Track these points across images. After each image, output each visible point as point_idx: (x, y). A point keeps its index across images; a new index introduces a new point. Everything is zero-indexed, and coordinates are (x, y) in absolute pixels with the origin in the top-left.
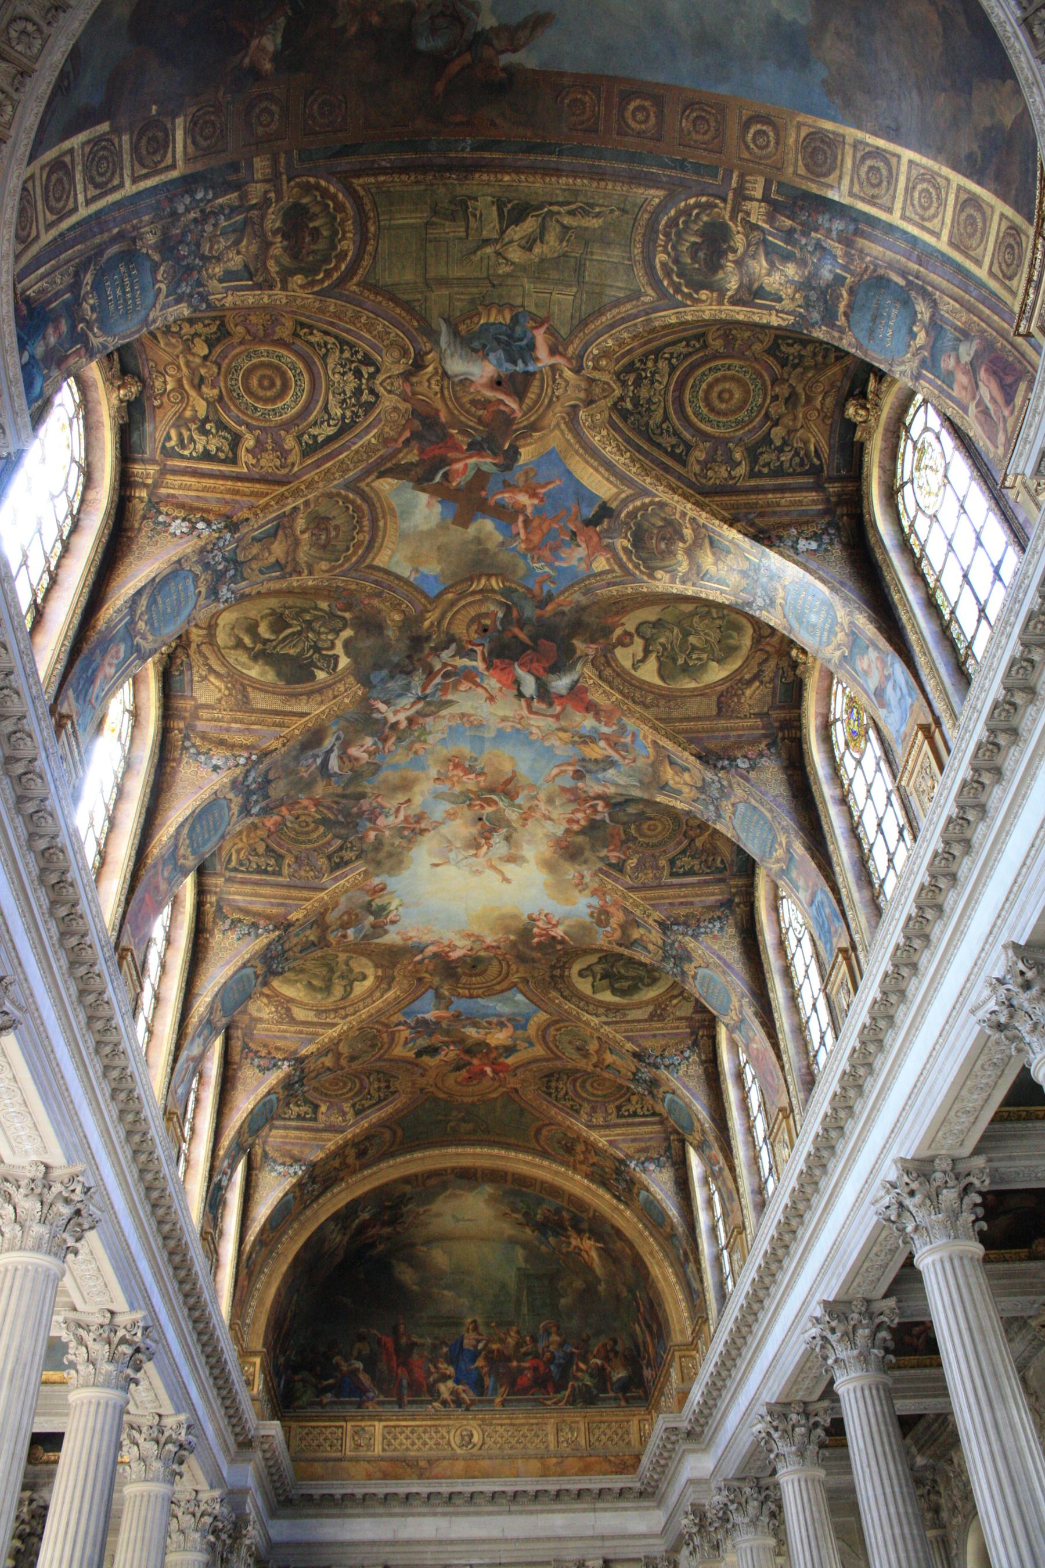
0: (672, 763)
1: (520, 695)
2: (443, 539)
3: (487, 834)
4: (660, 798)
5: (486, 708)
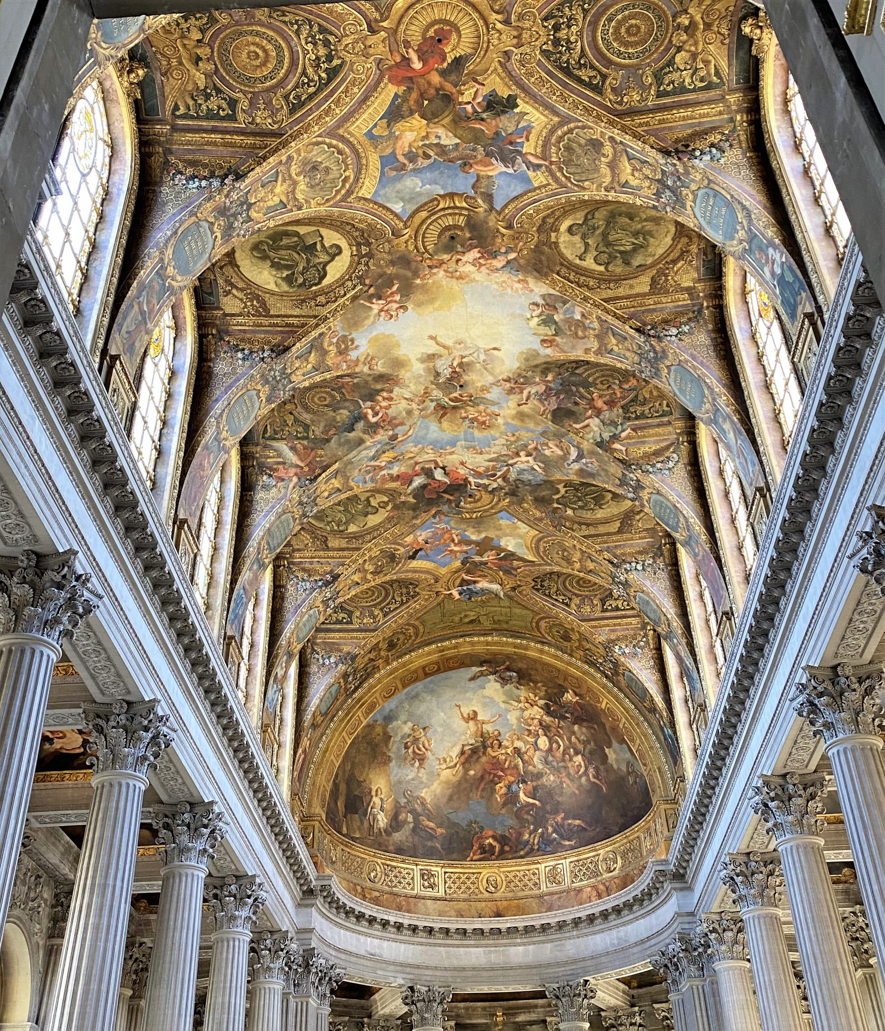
0: (339, 490)
1: (443, 468)
2: (498, 533)
3: (455, 376)
5: (467, 459)
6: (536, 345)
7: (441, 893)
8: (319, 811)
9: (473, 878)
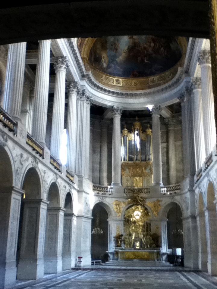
7: (121, 85)
9: (130, 82)
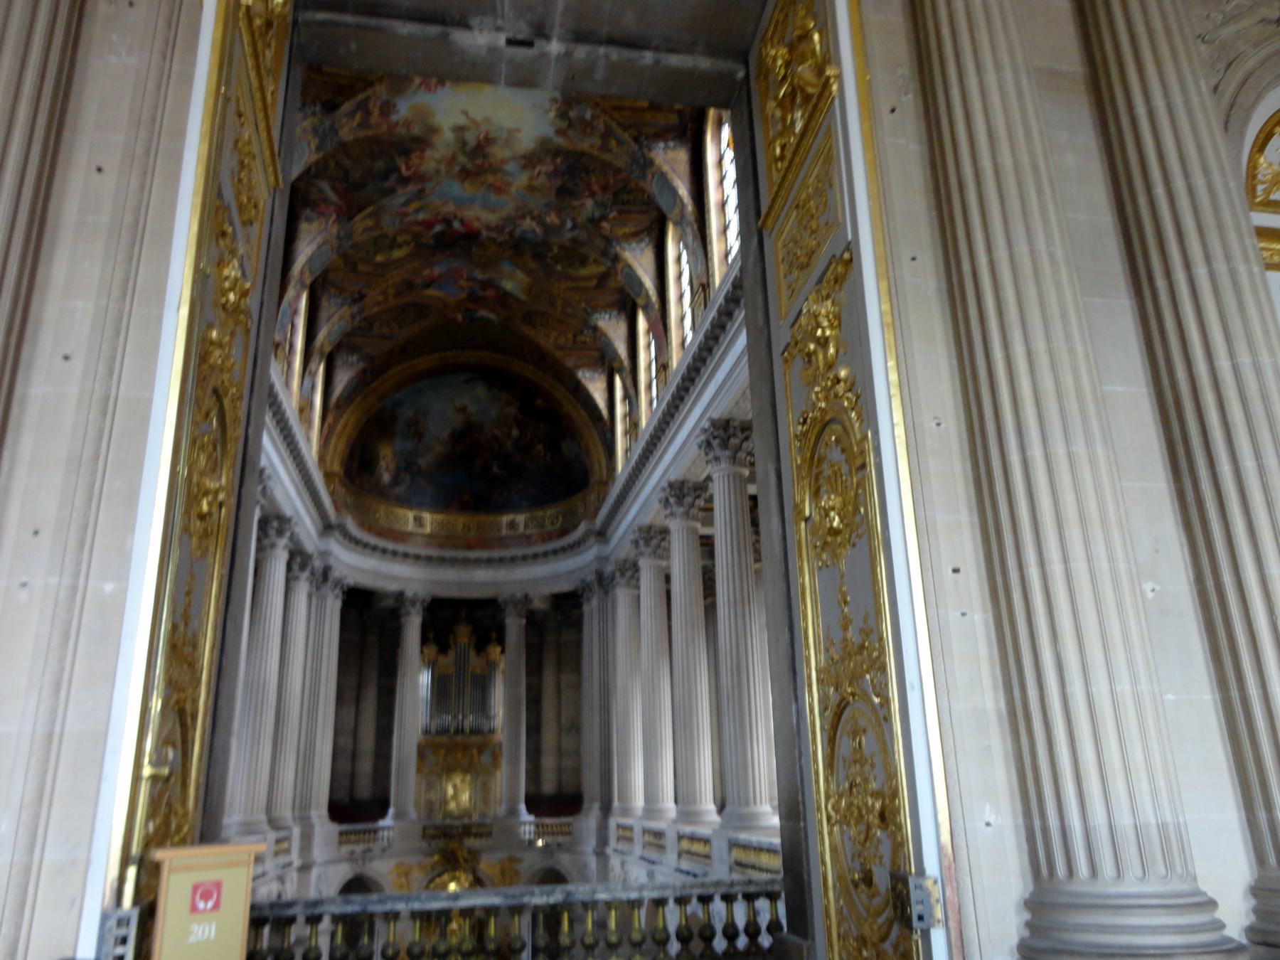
4: (371, 209)
6: (549, 132)
7: (428, 530)
8: (337, 468)
